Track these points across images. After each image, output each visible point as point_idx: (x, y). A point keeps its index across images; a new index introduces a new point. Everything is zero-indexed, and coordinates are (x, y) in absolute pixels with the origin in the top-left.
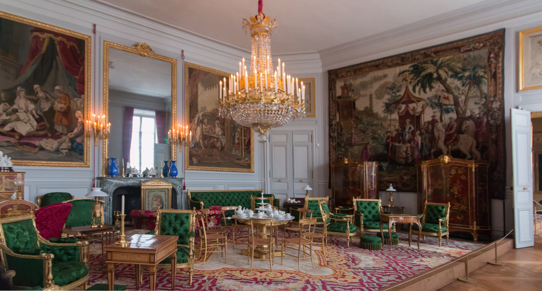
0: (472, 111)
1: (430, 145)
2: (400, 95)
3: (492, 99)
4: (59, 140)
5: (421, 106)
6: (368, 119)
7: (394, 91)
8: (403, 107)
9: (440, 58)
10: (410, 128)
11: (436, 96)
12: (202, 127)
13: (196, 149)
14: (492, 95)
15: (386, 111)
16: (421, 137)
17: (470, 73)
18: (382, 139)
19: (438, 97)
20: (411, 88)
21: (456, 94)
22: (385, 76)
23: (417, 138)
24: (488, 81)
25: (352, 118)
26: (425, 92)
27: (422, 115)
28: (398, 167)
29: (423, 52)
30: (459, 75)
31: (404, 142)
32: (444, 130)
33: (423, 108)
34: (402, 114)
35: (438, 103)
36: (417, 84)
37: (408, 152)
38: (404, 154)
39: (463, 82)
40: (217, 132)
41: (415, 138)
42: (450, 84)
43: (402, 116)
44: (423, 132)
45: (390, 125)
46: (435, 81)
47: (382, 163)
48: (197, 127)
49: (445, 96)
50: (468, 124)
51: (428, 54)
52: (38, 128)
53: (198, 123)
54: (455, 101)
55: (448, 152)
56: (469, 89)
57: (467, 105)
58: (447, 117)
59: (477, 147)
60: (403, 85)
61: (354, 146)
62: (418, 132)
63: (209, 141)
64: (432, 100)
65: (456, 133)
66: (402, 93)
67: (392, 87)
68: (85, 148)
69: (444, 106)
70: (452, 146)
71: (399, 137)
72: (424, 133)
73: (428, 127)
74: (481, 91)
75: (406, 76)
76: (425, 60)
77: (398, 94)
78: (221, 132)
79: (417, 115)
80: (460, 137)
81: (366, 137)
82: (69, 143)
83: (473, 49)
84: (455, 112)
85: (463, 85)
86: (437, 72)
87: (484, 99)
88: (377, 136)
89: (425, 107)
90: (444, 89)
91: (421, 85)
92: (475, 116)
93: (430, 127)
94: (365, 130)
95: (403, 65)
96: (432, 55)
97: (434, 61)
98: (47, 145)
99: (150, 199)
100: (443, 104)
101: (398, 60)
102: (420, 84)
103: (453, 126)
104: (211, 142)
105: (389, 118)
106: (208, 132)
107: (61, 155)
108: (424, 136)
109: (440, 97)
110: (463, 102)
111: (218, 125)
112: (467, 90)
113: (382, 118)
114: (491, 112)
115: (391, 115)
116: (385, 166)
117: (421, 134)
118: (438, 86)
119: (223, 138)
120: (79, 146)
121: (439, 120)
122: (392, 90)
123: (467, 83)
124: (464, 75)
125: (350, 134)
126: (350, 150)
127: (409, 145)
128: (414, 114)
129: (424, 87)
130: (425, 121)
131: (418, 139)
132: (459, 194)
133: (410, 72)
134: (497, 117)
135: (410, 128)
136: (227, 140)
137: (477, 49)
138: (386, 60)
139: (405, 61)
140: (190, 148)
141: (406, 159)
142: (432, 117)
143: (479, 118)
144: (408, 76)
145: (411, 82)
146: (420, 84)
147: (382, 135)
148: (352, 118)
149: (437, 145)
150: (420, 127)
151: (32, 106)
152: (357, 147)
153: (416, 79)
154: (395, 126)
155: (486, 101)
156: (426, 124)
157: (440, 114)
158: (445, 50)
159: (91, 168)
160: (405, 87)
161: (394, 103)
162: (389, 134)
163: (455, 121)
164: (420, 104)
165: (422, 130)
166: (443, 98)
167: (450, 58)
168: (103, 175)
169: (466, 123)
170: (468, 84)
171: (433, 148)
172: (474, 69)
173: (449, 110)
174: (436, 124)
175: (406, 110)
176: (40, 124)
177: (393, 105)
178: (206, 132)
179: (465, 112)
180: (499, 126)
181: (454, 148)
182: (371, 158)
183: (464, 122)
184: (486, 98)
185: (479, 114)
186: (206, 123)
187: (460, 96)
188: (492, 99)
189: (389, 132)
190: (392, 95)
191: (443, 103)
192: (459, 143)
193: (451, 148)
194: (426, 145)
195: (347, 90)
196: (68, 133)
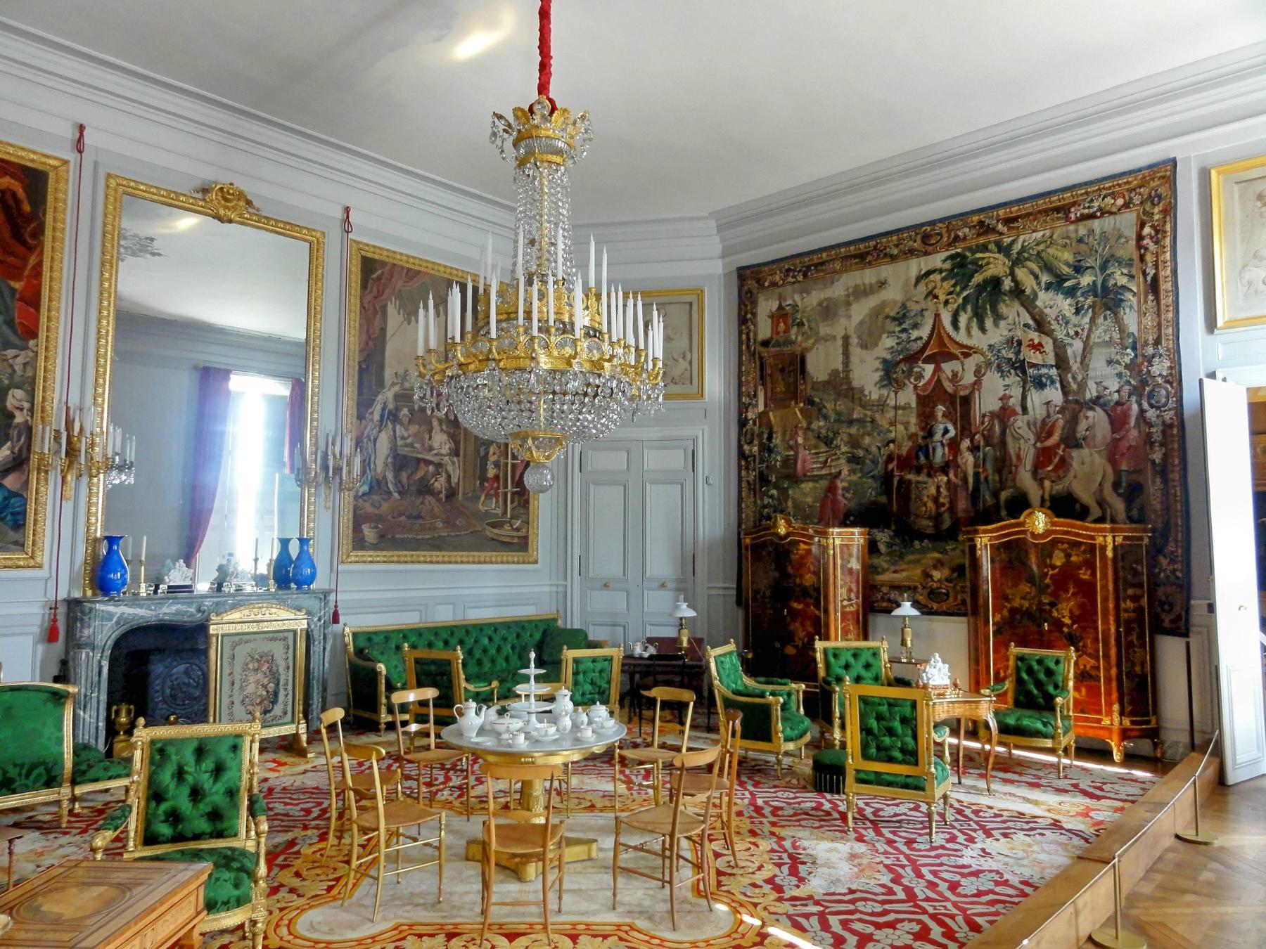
1: (997, 478)
2: (921, 338)
3: (1150, 350)
5: (973, 369)
7: (903, 326)
8: (929, 369)
9: (1018, 236)
10: (946, 431)
11: (1010, 341)
12: (394, 431)
13: (375, 497)
14: (1151, 341)
16: (974, 457)
18: (875, 463)
20: (946, 319)
21: (1060, 335)
22: (882, 284)
24: (1139, 302)
26: (983, 329)
27: (977, 392)
28: (917, 543)
29: (975, 219)
30: (1067, 284)
31: (931, 471)
32: (1032, 437)
33: (978, 373)
34: (924, 390)
35: (1016, 362)
36: (962, 307)
37: (942, 500)
38: (930, 504)
39: (1077, 303)
40: (436, 445)
43: (925, 397)
45: (893, 423)
46: (1006, 298)
47: (875, 531)
48: (380, 431)
49: (1032, 340)
50: (1091, 420)
54: (1057, 355)
56: (1093, 320)
58: (1036, 399)
59: (1116, 486)
62: (966, 443)
63: (412, 474)
64: (999, 351)
65: (1062, 446)
66: (924, 332)
67: (900, 315)
68: (31, 507)
70: (1053, 482)
71: (917, 458)
72: (982, 443)
73: (991, 429)
74: (1122, 330)
76: (982, 240)
77: (915, 334)
78: (447, 446)
79: (962, 393)
80: (1072, 458)
84: (1058, 385)
85: (1077, 312)
86: (1012, 273)
87: (1129, 351)
88: (861, 453)
90: (1031, 322)
93: (997, 429)
95: (926, 253)
96: (1000, 227)
99: (238, 668)
102: (969, 308)
103: (1053, 425)
104: (418, 475)
106: (412, 445)
108: (981, 454)
109: (1020, 343)
110: (1079, 360)
111: (441, 424)
112: (1087, 326)
114: (1148, 385)
116: (884, 539)
117: (974, 449)
118: (1013, 311)
119: (453, 463)
120: (12, 501)
121: (1019, 410)
122: (900, 324)
124: (1079, 284)
128: (956, 391)
129: (979, 316)
130: (983, 412)
133: (944, 274)
134: (1164, 400)
135: (946, 431)
136: (465, 472)
140: (356, 498)
141: (937, 518)
142: (1001, 399)
143: (1118, 403)
144: (939, 284)
145: (946, 303)
146: (969, 308)
147: (874, 449)
149: (1014, 480)
153: (958, 295)
154: (906, 424)
155: (1136, 356)
156: (986, 419)
158: (1031, 214)
162: (892, 445)
164: (972, 362)
166: (1029, 346)
167: (1043, 235)
168: (84, 592)
169: (1087, 418)
172: (1104, 267)
173: (1044, 380)
174: (1012, 419)
177: (904, 367)
178: (406, 446)
179: (1082, 386)
180: (1171, 426)
181: (1059, 487)
184: (1134, 348)
185: (1118, 391)
186: (406, 420)
187: (1070, 341)
188: (1150, 350)
189: (893, 441)
190: (898, 338)
191: (1027, 360)
192: (1071, 474)
193: (1051, 489)
194: (986, 478)
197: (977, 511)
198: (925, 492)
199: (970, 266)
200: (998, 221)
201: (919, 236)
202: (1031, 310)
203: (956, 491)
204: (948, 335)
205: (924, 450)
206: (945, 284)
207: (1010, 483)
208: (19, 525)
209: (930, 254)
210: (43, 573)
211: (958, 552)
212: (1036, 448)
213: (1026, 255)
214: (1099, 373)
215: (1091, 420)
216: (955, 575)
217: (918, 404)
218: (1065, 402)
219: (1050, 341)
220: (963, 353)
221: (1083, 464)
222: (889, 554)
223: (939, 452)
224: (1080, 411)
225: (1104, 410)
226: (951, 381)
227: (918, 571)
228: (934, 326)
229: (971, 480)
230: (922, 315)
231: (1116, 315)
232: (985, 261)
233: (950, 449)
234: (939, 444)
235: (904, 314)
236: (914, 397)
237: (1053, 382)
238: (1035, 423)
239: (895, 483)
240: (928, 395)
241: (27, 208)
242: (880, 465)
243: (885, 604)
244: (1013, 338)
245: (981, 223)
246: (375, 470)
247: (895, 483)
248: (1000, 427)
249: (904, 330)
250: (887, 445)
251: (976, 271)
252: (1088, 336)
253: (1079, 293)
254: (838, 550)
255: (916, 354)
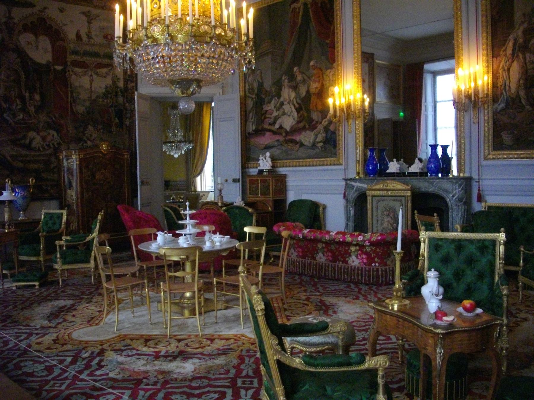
4: (315, 131)
48: (513, 62)
52: (298, 120)
53: (513, 54)
82: (323, 133)
98: (306, 139)
107: (317, 150)
140: (495, 113)
151: (293, 95)
159: (342, 167)
176: (299, 115)
196: (323, 119)
208: (335, 147)
210: (342, 167)
241: (328, 6)
246: (510, 91)
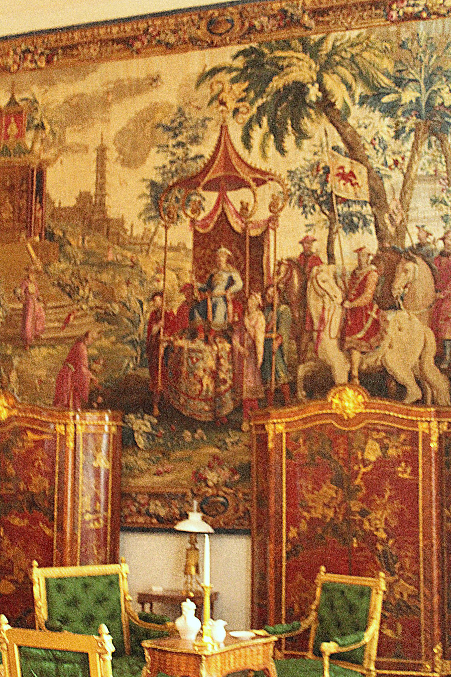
0: (423, 226)
1: (294, 347)
2: (202, 156)
5: (269, 201)
6: (87, 238)
7: (180, 139)
9: (328, 33)
10: (231, 282)
15: (152, 214)
16: (266, 319)
17: (418, 95)
18: (136, 324)
19: (321, 172)
21: (376, 164)
23: (253, 323)
25: (29, 235)
26: (281, 150)
27: (271, 232)
28: (187, 433)
30: (385, 99)
32: (339, 294)
35: (322, 195)
37: (222, 375)
38: (207, 381)
39: (397, 124)
41: (246, 321)
42: (359, 127)
43: (207, 235)
44: (273, 298)
45: (161, 270)
46: (312, 112)
47: (132, 417)
49: (342, 168)
50: (410, 275)
51: (292, 15)
54: (371, 188)
55: (350, 377)
57: (408, 204)
60: (210, 119)
61: (33, 347)
64: (301, 179)
65: (376, 307)
67: (176, 124)
69: (340, 203)
70: (363, 353)
71: (192, 317)
72: (276, 301)
73: (288, 282)
75: (220, 86)
76: (283, 34)
77: (194, 150)
79: (253, 233)
80: (387, 322)
81: (80, 313)
83: (424, 15)
84: (372, 227)
85: (397, 136)
86: (320, 81)
88: (116, 308)
89: (280, 205)
90: (342, 145)
91: (269, 124)
92: (433, 247)
94: (76, 282)
95: (211, 45)
97: (312, 42)
100: (337, 197)
101: (199, 28)
102: (265, 120)
103: (366, 279)
105: (160, 241)
109: (327, 170)
110: (398, 196)
112: (408, 154)
113: (136, 238)
115: (166, 228)
116: (144, 428)
121: (324, 258)
122: (175, 136)
123: (407, 129)
124: (400, 100)
125: (19, 299)
126: (15, 361)
127: (227, 346)
128: (245, 230)
130: (279, 259)
131: (254, 327)
132: (389, 536)
133: (234, 74)
135: (231, 282)
137: (439, 15)
138: (158, 23)
139: (221, 34)
142: (302, 243)
145: (236, 111)
146: (265, 120)
147: (135, 305)
148: (29, 235)
149: (316, 351)
150: (262, 284)
152: (44, 350)
153: (252, 103)
154: (177, 271)
156: (283, 268)
157: (327, 231)
160: (219, 128)
161: (182, 183)
162: (158, 299)
163: (373, 263)
165: (270, 291)
166: (338, 175)
167: (359, 36)
169: (406, 271)
170: (411, 130)
171: (303, 363)
172: (429, 82)
173: (355, 219)
174: (315, 269)
175: (219, 211)
182: (92, 396)
183: (400, 266)
185: (443, 239)
187: (389, 172)
189: (161, 294)
190: (173, 154)
191: (336, 193)
192: (385, 344)
193: (361, 363)
194: (280, 347)
195: (18, 126)
197: (267, 391)
198: (201, 364)
199: (268, 67)
200: (304, 12)
201: (204, 22)
202: (342, 130)
203: (241, 363)
204: (237, 154)
205: (201, 307)
206: (235, 86)
207: (309, 354)
209: (216, 46)
211: (241, 447)
212: (343, 308)
213: (337, 58)
214: (421, 215)
215: (410, 275)
216: (237, 477)
217: (195, 245)
218: (380, 249)
219: (365, 170)
220: (254, 180)
221: (400, 329)
222: (149, 449)
223: (221, 310)
224: (398, 262)
225: (426, 262)
226: (238, 215)
227: (188, 473)
228: (219, 141)
229: (260, 348)
230: (204, 126)
231: (442, 142)
232: (285, 63)
233: (235, 307)
234: (221, 299)
235: (181, 124)
236: (190, 235)
237: (366, 224)
238: (343, 275)
239: (162, 350)
240: (209, 233)
242: (142, 327)
243: (141, 520)
244: (318, 163)
245: (283, 12)
247: (162, 350)
248: (299, 280)
249: (180, 145)
250: (153, 298)
251: (276, 74)
252: (410, 167)
253: (400, 112)
254: (80, 441)
255: (196, 176)
